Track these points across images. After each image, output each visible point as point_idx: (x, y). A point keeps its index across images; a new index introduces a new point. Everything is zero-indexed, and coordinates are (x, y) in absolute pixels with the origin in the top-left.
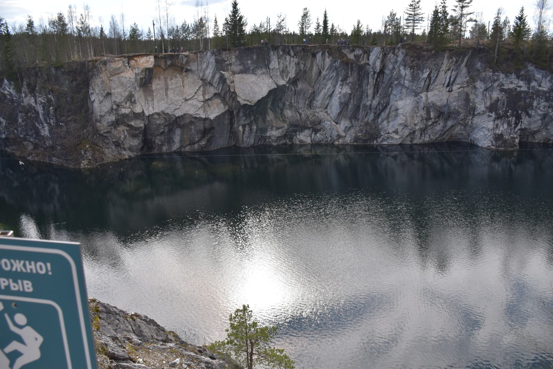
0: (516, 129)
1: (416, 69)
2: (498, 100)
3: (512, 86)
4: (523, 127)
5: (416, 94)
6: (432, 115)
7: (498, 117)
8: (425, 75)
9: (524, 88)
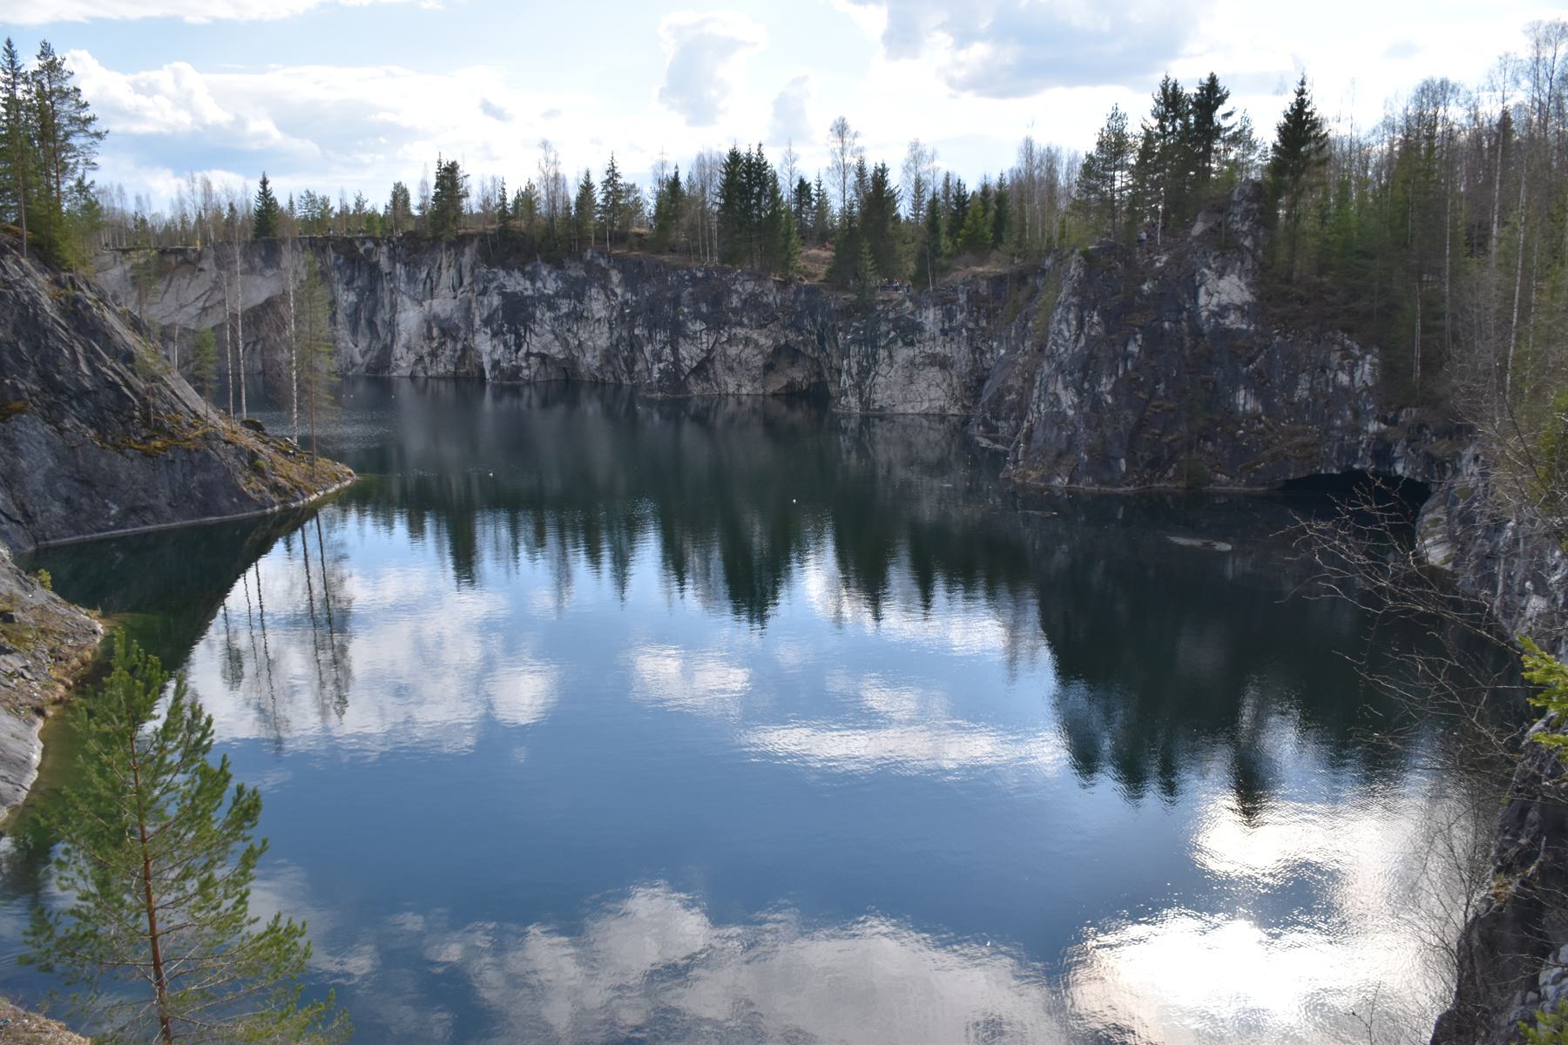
0: (521, 353)
1: (412, 265)
2: (496, 310)
3: (519, 288)
4: (535, 351)
5: (420, 304)
6: (435, 332)
7: (494, 335)
8: (424, 275)
9: (530, 292)
